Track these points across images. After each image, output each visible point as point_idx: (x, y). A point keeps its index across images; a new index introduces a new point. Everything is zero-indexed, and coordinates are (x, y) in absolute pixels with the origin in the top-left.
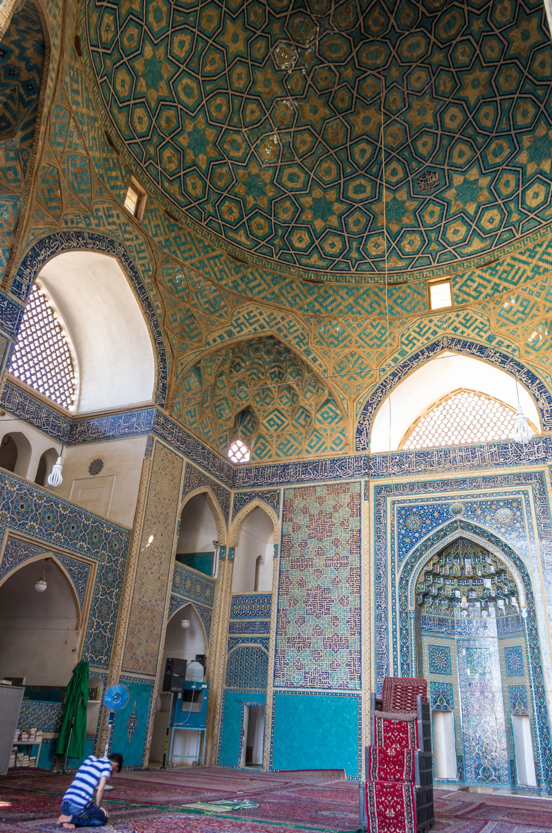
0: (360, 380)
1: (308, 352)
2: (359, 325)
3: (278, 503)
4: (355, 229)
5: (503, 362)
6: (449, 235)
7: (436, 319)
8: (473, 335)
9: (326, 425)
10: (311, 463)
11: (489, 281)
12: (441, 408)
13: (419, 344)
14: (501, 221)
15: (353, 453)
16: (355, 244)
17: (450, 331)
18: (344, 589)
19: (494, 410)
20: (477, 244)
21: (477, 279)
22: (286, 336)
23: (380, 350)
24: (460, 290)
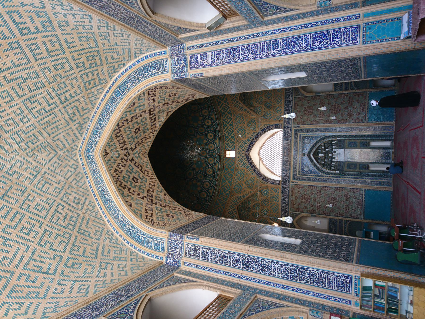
0: (255, 181)
1: (244, 196)
2: (236, 180)
3: (295, 214)
4: (203, 177)
5: (257, 137)
6: (212, 149)
7: (238, 156)
8: (246, 145)
9: (269, 194)
10: (282, 201)
11: (230, 139)
13: (246, 162)
14: (212, 133)
15: (280, 186)
16: (208, 178)
17: (243, 152)
18: (329, 192)
20: (217, 141)
22: (238, 203)
23: (245, 174)
24: (230, 148)
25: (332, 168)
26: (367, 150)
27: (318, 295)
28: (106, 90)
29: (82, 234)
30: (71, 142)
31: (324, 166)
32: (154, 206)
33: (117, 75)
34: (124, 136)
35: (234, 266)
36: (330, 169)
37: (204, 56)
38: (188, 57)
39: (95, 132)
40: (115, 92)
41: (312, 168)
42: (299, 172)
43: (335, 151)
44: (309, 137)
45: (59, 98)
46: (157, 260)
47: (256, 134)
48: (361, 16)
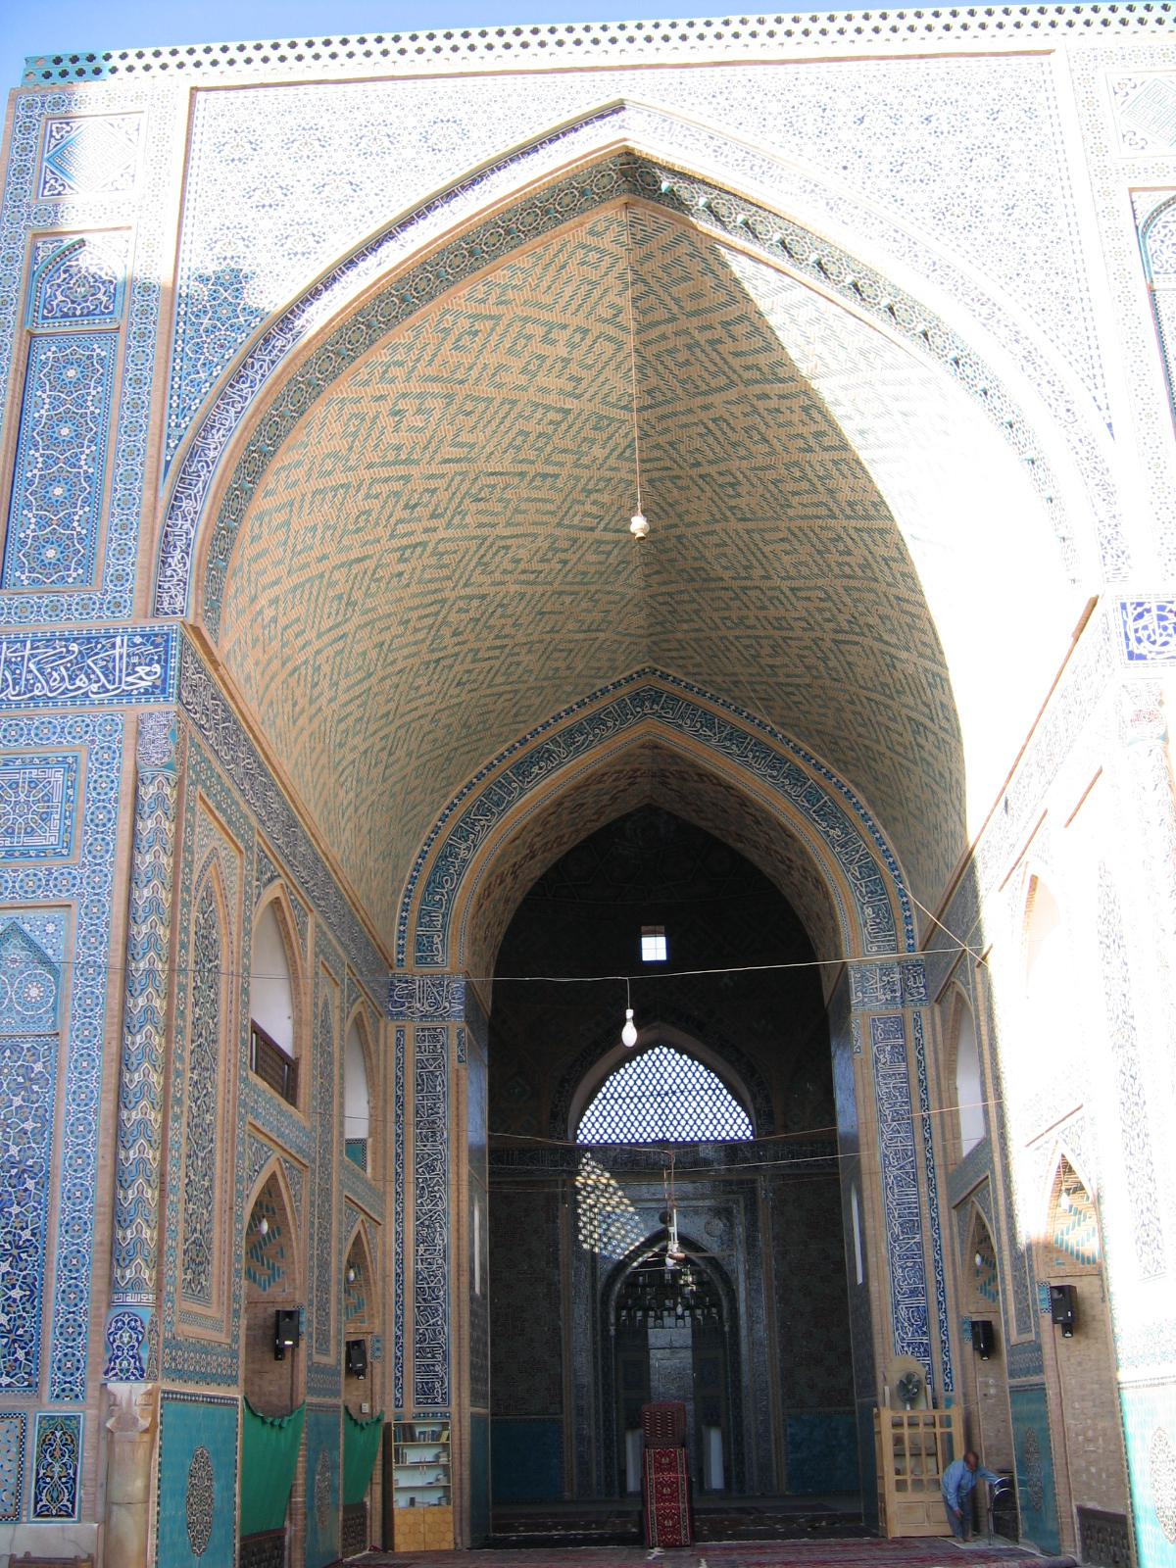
12: (634, 1064)
19: (698, 1075)
25: (624, 1313)
28: (822, 760)
30: (681, 662)
32: (509, 879)
33: (860, 798)
34: (701, 786)
35: (420, 1158)
39: (709, 720)
48: (950, 1393)
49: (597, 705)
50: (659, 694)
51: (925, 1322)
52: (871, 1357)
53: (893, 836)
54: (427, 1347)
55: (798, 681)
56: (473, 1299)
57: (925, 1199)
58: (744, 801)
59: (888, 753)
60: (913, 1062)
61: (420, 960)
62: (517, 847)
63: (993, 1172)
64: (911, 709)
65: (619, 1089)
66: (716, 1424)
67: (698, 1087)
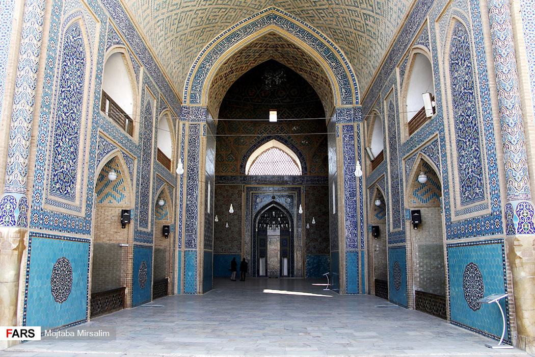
7: (271, 126)
20: (288, 100)
21: (287, 113)
26: (279, 256)
27: (180, 228)
28: (330, 40)
29: (202, 32)
30: (283, 4)
31: (263, 216)
32: (224, 79)
34: (289, 49)
36: (259, 223)
37: (352, 137)
38: (352, 124)
39: (293, 26)
40: (328, 49)
41: (259, 208)
42: (255, 193)
43: (278, 227)
44: (292, 202)
45: (321, 9)
46: (183, 98)
47: (296, 146)
49: (255, 19)
50: (276, 16)
51: (356, 226)
52: (337, 237)
53: (354, 65)
54: (190, 229)
55: (324, 7)
56: (206, 214)
57: (358, 186)
58: (303, 54)
59: (354, 31)
60: (356, 140)
61: (191, 102)
62: (226, 67)
63: (387, 173)
64: (365, 9)
65: (262, 160)
66: (286, 257)
67: (285, 160)
